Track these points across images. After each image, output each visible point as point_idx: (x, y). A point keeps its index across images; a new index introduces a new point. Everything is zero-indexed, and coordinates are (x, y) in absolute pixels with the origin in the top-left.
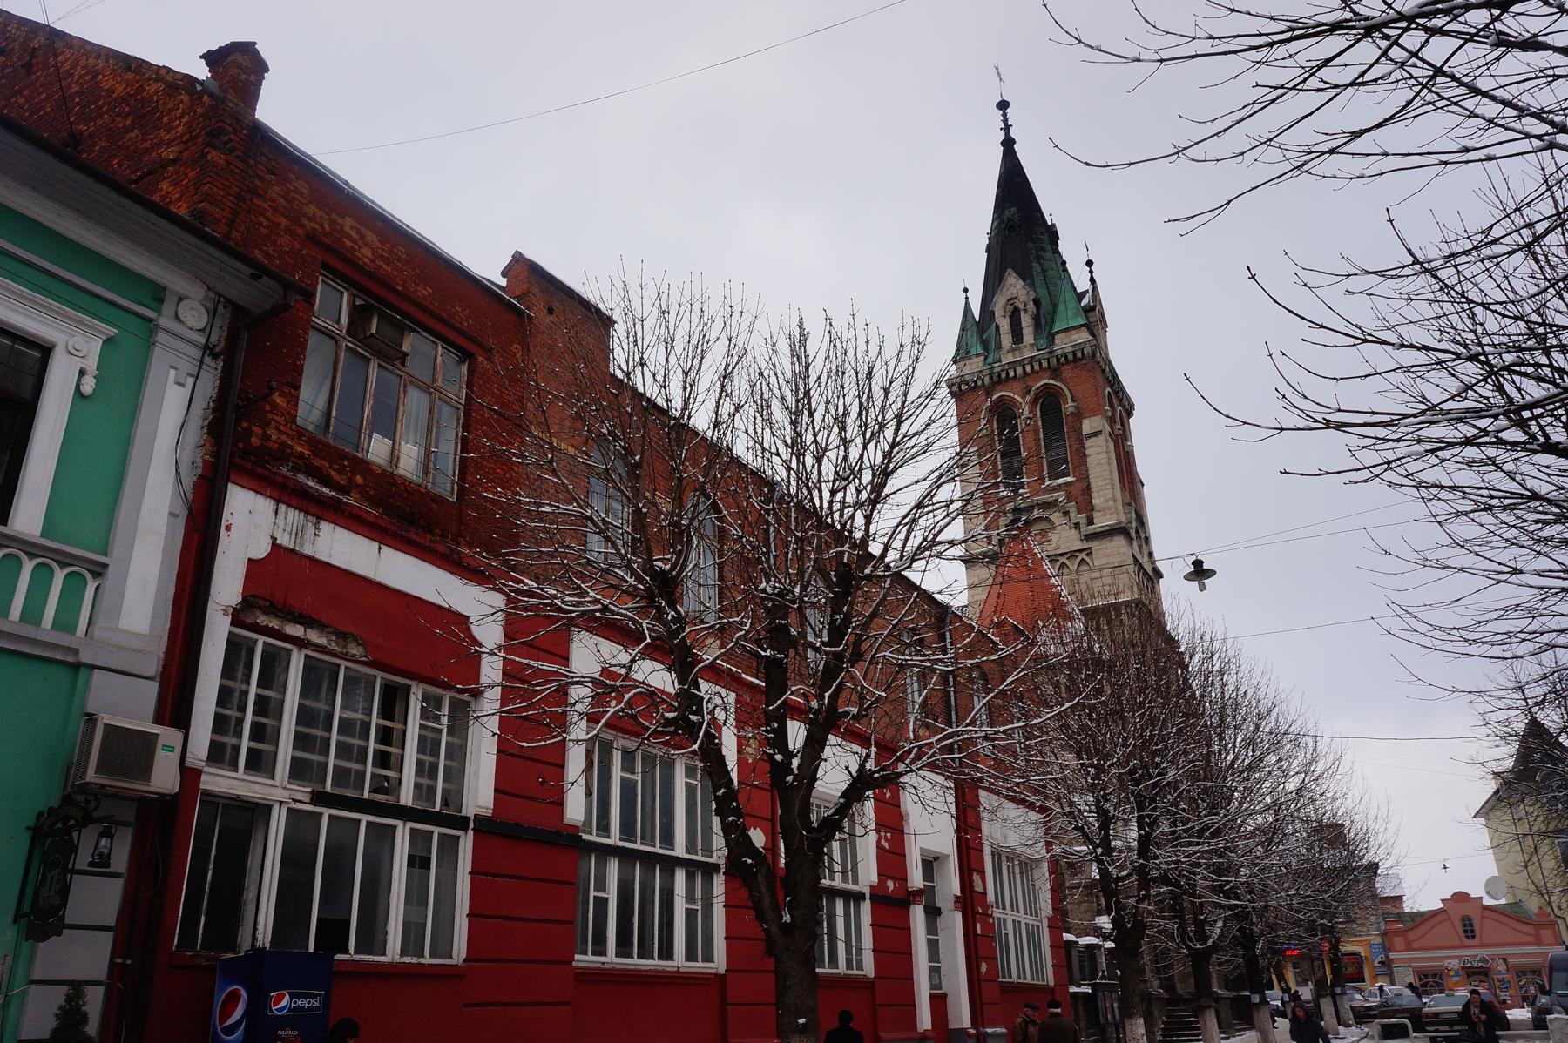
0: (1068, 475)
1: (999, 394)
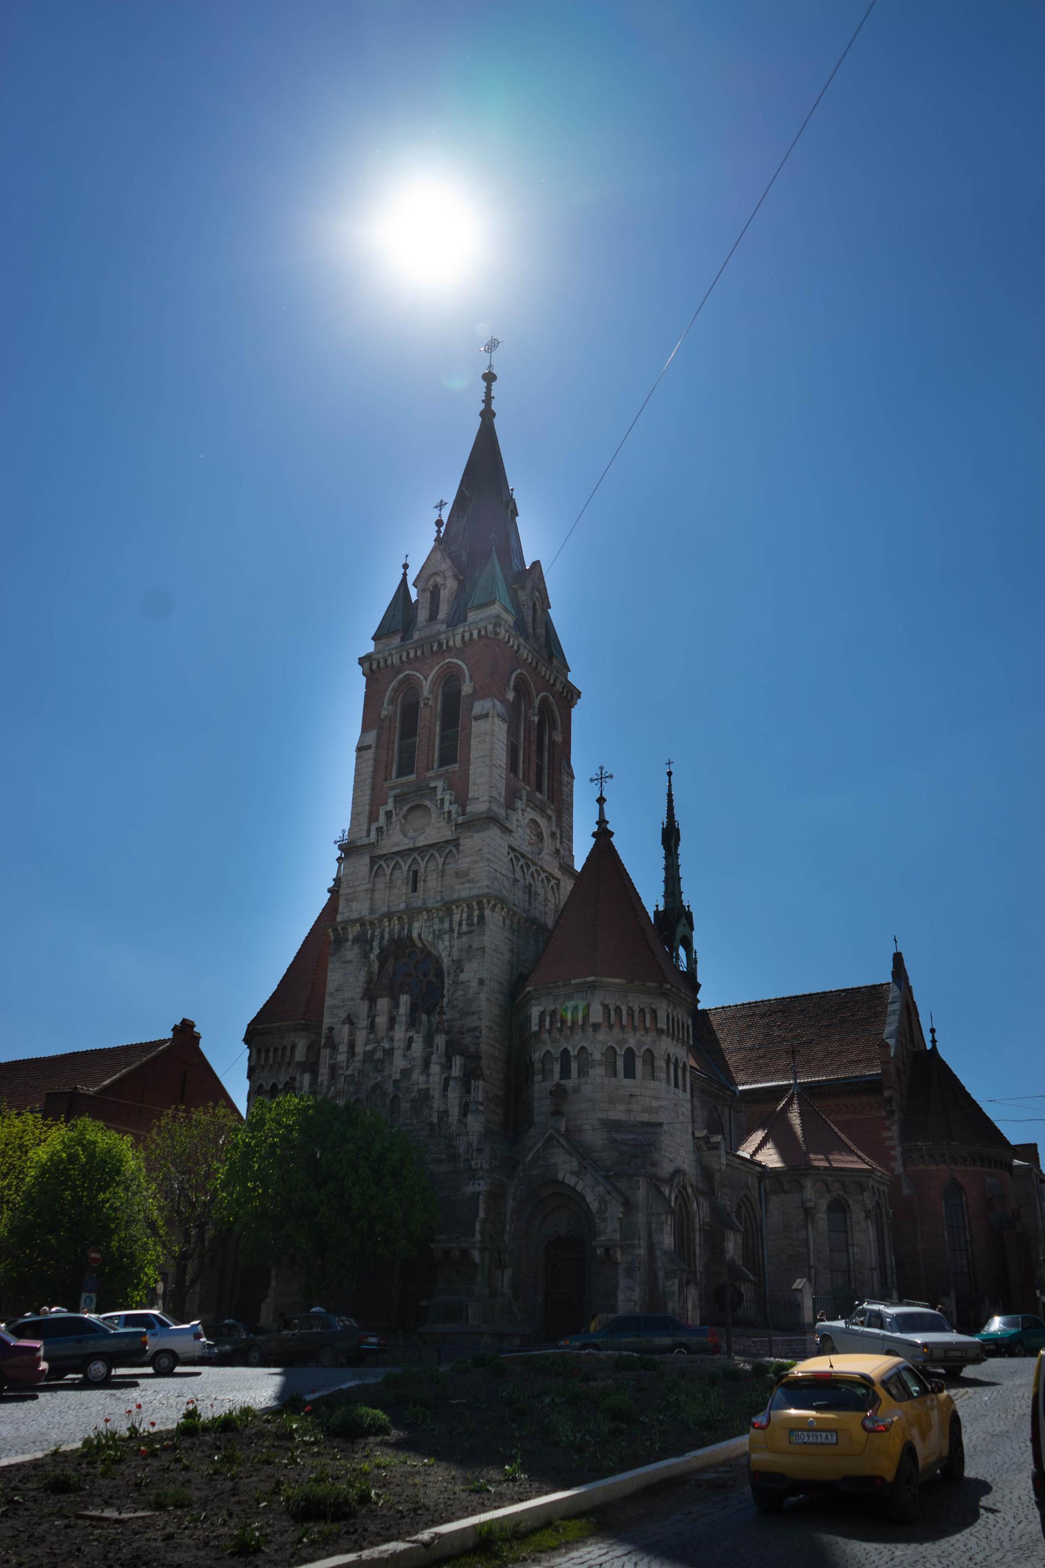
1: (407, 672)
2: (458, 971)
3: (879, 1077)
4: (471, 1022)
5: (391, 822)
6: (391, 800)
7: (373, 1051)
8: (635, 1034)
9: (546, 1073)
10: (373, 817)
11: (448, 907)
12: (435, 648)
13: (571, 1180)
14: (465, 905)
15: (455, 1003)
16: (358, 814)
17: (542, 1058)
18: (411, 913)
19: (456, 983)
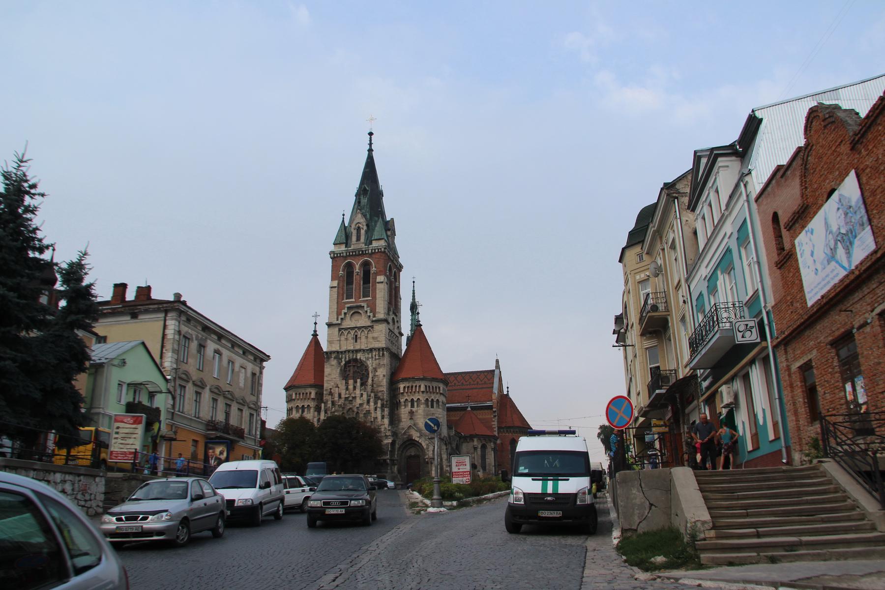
4: (380, 389)
6: (346, 309)
7: (348, 397)
9: (405, 406)
10: (339, 314)
11: (371, 350)
12: (361, 253)
13: (417, 439)
18: (357, 351)
19: (375, 375)
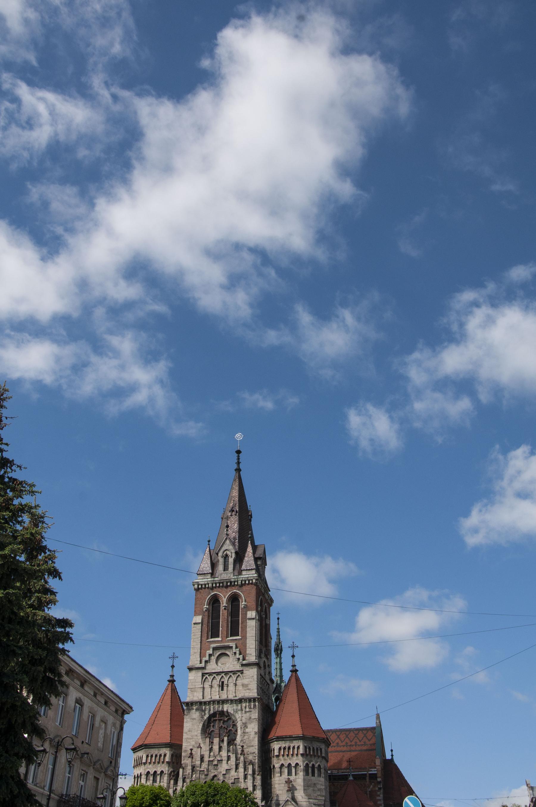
0: (239, 636)
1: (216, 593)
2: (245, 728)
3: (376, 772)
5: (211, 659)
6: (211, 649)
7: (212, 761)
8: (315, 758)
11: (240, 701)
12: (229, 584)
14: (248, 700)
15: (244, 741)
16: (195, 653)
17: (280, 766)
18: (224, 702)
19: (243, 732)
